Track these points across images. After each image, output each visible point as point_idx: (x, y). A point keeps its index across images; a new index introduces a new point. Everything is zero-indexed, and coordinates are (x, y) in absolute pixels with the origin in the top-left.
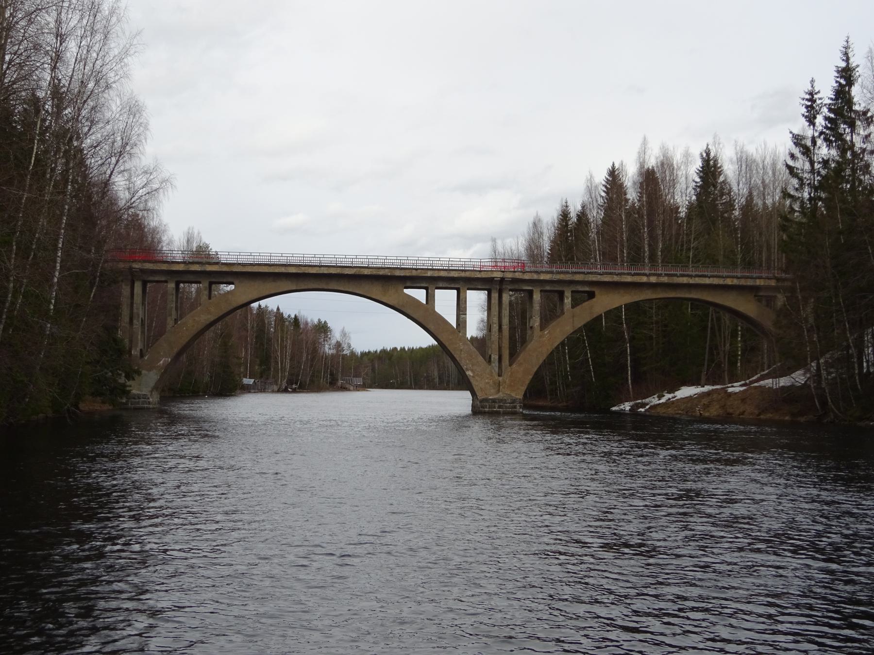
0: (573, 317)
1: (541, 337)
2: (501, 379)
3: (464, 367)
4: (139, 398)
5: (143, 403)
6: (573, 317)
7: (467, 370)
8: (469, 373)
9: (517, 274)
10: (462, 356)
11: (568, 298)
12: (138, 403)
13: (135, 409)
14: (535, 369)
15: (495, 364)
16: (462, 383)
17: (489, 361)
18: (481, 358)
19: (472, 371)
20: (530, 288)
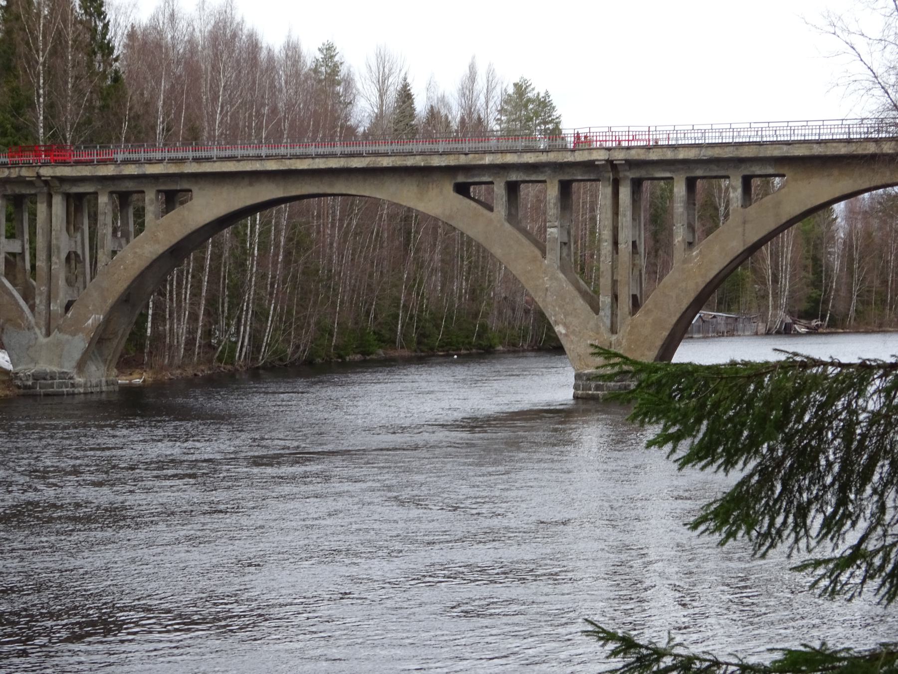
0: (744, 222)
1: (685, 261)
2: (614, 338)
3: (552, 320)
4: (52, 378)
5: (60, 385)
6: (744, 222)
7: (556, 323)
8: (560, 329)
9: (633, 152)
10: (549, 299)
11: (735, 189)
12: (52, 386)
13: (47, 395)
14: (674, 320)
15: (606, 312)
16: (550, 347)
17: (596, 308)
18: (580, 303)
19: (566, 326)
20: (668, 175)
